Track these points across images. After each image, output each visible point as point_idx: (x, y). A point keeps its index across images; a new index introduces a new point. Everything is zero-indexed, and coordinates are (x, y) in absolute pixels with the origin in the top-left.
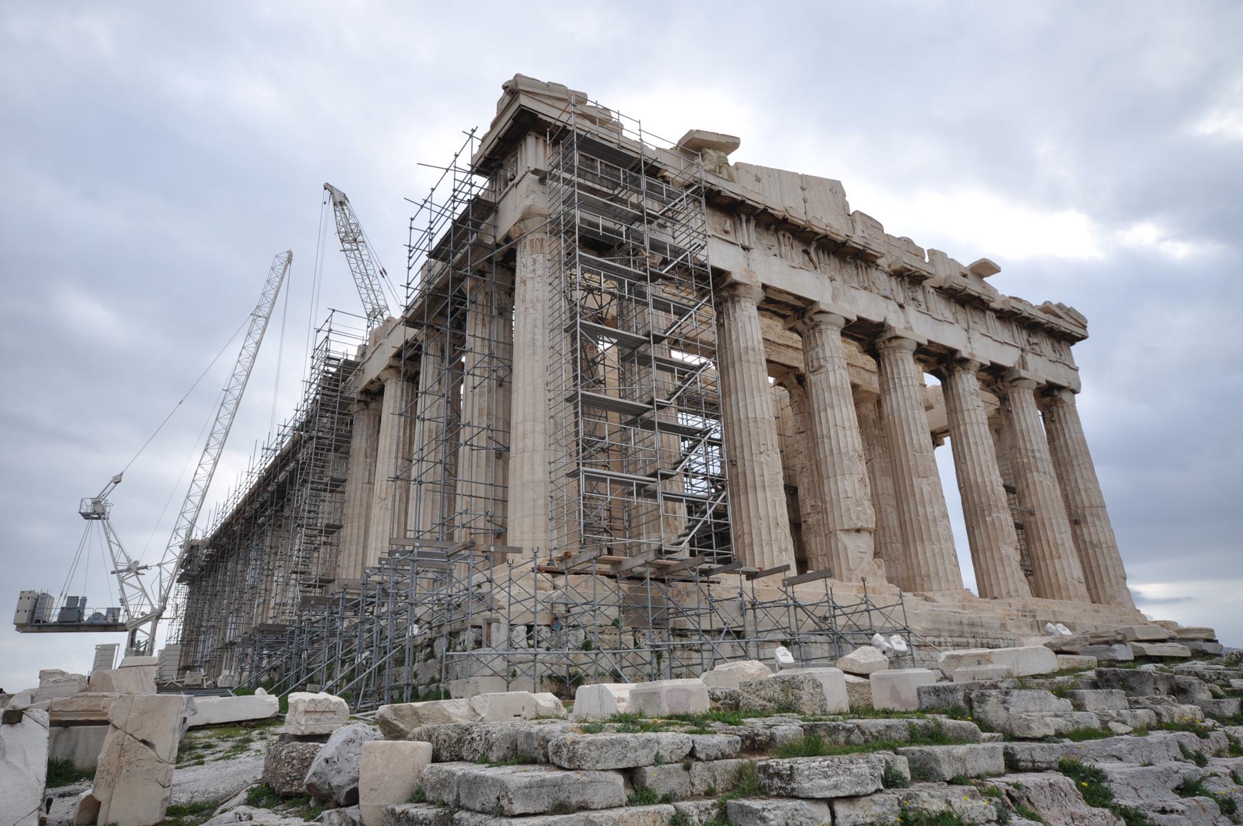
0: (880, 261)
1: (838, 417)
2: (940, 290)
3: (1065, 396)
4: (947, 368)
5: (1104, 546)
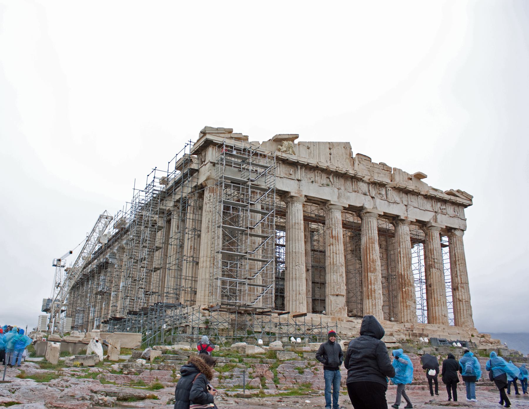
0: (363, 179)
1: (334, 249)
2: (394, 188)
3: (457, 233)
4: (396, 222)
5: (464, 301)
